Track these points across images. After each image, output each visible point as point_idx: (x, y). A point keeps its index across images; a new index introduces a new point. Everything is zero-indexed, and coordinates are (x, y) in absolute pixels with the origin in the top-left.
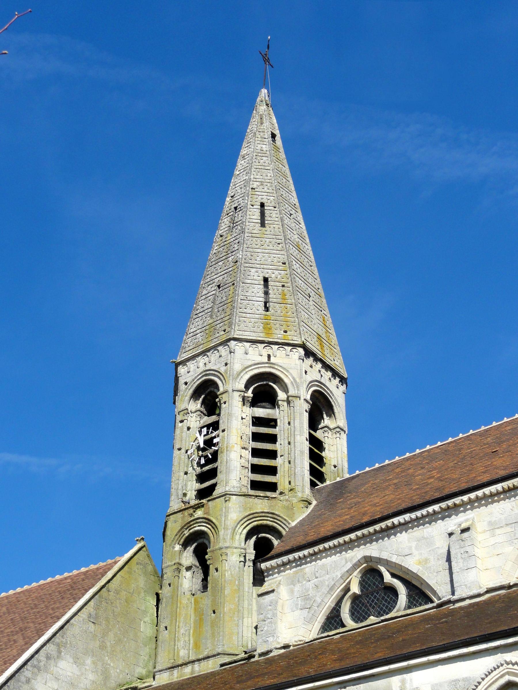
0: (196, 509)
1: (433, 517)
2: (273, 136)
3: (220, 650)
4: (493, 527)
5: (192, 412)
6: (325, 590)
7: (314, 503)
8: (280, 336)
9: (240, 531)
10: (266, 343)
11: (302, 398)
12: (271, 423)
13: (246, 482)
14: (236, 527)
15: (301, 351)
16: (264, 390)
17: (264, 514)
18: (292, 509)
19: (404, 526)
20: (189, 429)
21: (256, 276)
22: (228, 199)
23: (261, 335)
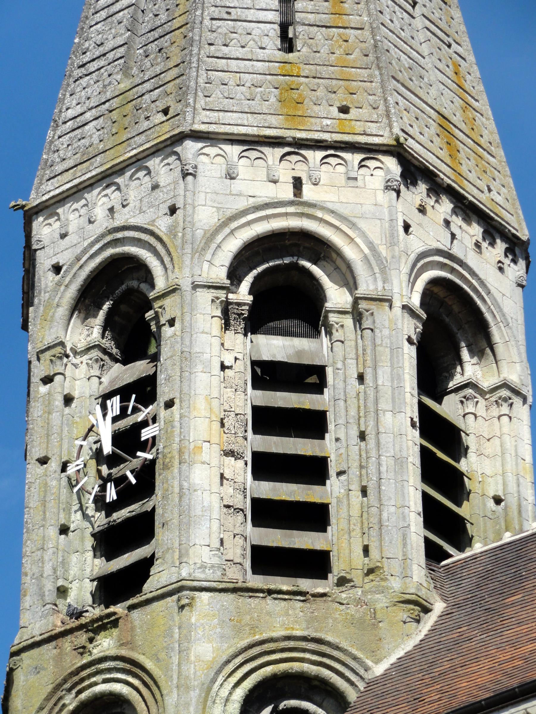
0: (97, 631)
5: (76, 353)
7: (439, 607)
8: (329, 122)
9: (224, 692)
10: (289, 144)
11: (397, 304)
12: (309, 377)
13: (239, 551)
14: (213, 681)
15: (392, 166)
16: (284, 281)
17: (292, 644)
18: (375, 626)
20: (68, 400)
23: (274, 120)
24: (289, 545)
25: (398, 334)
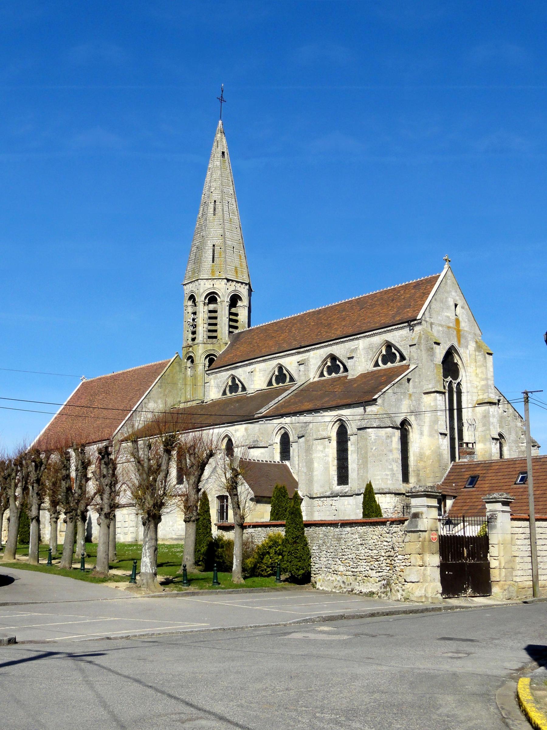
1: (247, 365)
2: (223, 153)
3: (196, 398)
4: (260, 370)
6: (222, 383)
7: (229, 343)
12: (216, 312)
13: (206, 337)
15: (225, 281)
16: (212, 298)
19: (240, 367)
21: (210, 245)
22: (203, 196)
24: (212, 335)
25: (226, 305)
